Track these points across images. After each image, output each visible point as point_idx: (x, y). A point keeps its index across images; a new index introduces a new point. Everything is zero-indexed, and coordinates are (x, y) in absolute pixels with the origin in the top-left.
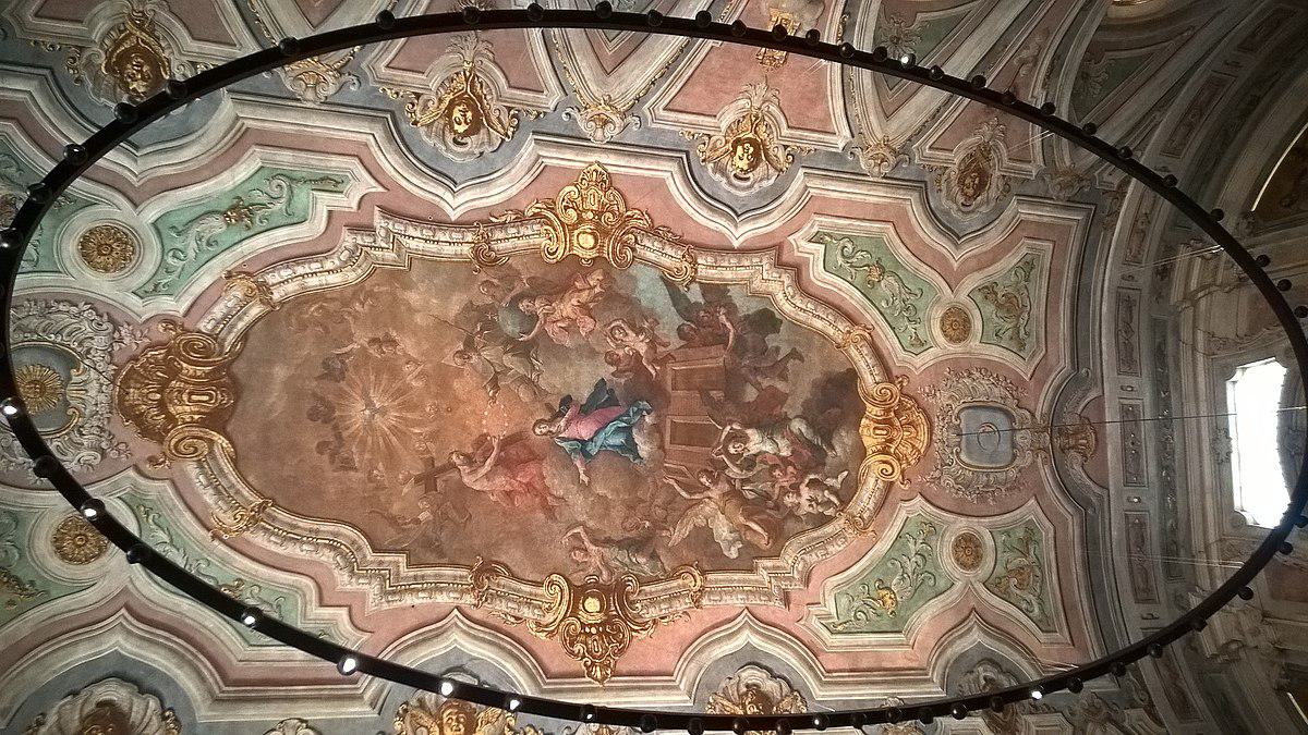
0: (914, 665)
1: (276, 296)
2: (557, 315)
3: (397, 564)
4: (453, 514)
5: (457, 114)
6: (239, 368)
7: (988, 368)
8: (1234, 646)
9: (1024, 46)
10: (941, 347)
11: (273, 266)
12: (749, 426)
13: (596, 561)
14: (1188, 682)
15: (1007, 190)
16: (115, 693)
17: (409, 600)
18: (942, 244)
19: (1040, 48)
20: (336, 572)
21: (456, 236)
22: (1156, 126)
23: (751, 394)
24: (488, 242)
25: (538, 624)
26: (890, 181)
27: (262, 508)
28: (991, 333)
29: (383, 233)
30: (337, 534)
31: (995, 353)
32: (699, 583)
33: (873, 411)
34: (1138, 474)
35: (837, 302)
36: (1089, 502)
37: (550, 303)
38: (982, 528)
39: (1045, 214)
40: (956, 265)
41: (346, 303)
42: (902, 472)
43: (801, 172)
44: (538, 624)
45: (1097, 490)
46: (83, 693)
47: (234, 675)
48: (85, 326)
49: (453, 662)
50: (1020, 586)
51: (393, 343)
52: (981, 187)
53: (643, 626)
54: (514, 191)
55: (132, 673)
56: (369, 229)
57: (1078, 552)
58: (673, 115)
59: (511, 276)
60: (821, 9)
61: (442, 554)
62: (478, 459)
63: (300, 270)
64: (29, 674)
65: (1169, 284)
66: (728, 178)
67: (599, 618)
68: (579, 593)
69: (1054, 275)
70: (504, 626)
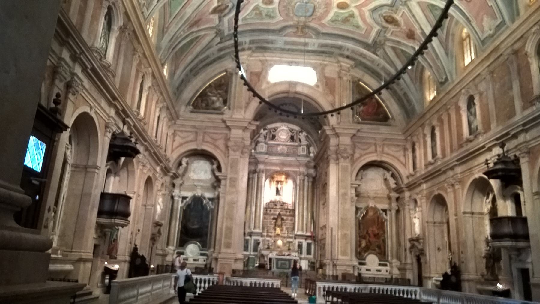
7: (327, 13)
15: (384, 27)
31: (331, 15)
45: (284, 34)
52: (387, 21)
69: (353, 33)
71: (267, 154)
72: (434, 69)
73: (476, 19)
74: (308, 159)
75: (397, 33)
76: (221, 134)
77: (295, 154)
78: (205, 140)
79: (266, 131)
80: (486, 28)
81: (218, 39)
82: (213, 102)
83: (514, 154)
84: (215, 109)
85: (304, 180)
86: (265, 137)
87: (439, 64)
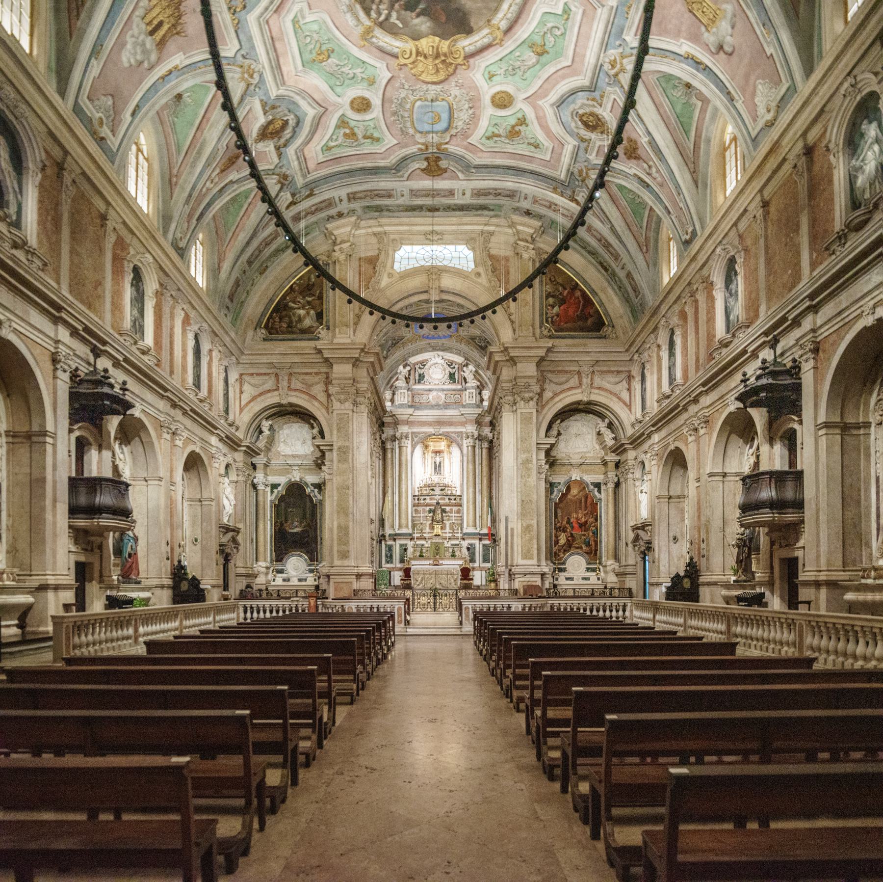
0: (286, 78)
9: (658, 171)
10: (488, 91)
15: (582, 140)
18: (554, 96)
26: (598, 69)
28: (498, 121)
33: (445, 46)
35: (520, 21)
36: (399, 171)
38: (376, 112)
39: (566, 159)
40: (540, 103)
42: (405, 65)
50: (345, 135)
52: (586, 125)
57: (370, 165)
60: (713, 50)
65: (521, 215)
69: (530, 159)
71: (410, 407)
73: (743, 91)
74: (479, 411)
76: (316, 374)
77: (458, 404)
78: (292, 387)
79: (408, 368)
82: (300, 320)
83: (790, 358)
84: (303, 331)
85: (474, 447)
86: (407, 379)
87: (681, 205)
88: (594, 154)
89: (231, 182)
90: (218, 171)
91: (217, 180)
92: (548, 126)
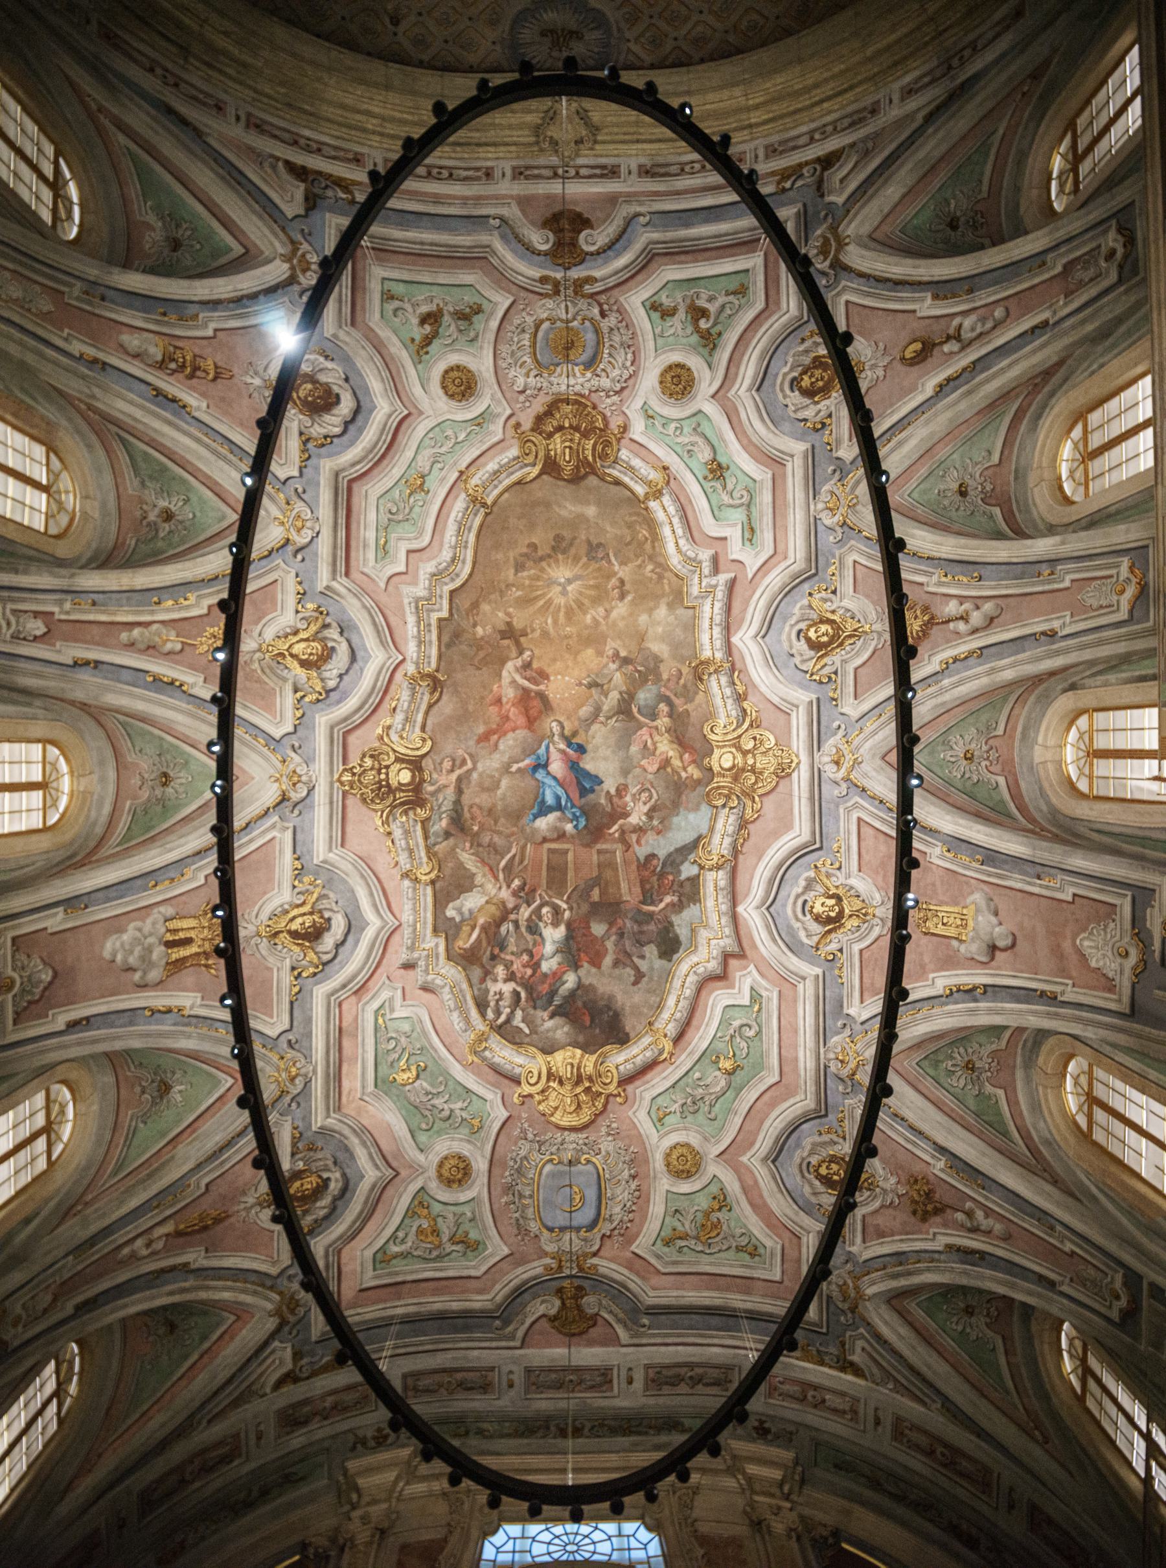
0: (344, 1099)
1: (653, 505)
2: (657, 738)
3: (440, 610)
4: (481, 654)
5: (824, 628)
6: (592, 481)
7: (641, 1197)
8: (354, 1497)
9: (988, 1212)
10: (660, 1144)
11: (677, 499)
12: (569, 926)
13: (443, 780)
14: (319, 1431)
16: (346, 406)
17: (411, 619)
18: (764, 1143)
19: (988, 1233)
20: (434, 563)
21: (718, 644)
22: (924, 1404)
23: (598, 929)
24: (716, 671)
25: (389, 727)
26: (822, 1074)
27: (484, 505)
28: (678, 1205)
29: (714, 582)
30: (464, 562)
31: (657, 1208)
32: (424, 878)
33: (589, 1064)
34: (540, 1387)
35: (694, 1022)
36: (507, 1322)
37: (668, 731)
38: (477, 1188)
40: (744, 1159)
41: (651, 558)
42: (530, 1096)
43: (819, 971)
44: (389, 727)
46: (346, 385)
47: (355, 486)
48: (617, 372)
49: (360, 654)
50: (420, 1231)
51: (622, 597)
53: (386, 822)
54: (763, 689)
55: (360, 418)
56: (716, 570)
57: (455, 1306)
58: (854, 828)
59: (688, 694)
60: (984, 959)
61: (448, 646)
62: (528, 673)
63: (676, 520)
64: (363, 353)
66: (803, 893)
67: (394, 783)
68: (415, 764)
69: (745, 1284)
70: (388, 698)
72: (1065, 1288)
73: (1063, 972)
75: (880, 1220)
80: (1110, 965)
81: (283, 1355)
87: (1068, 1247)
88: (859, 1239)
89: (185, 1269)
90: (168, 1228)
91: (159, 1245)
92: (765, 1204)
